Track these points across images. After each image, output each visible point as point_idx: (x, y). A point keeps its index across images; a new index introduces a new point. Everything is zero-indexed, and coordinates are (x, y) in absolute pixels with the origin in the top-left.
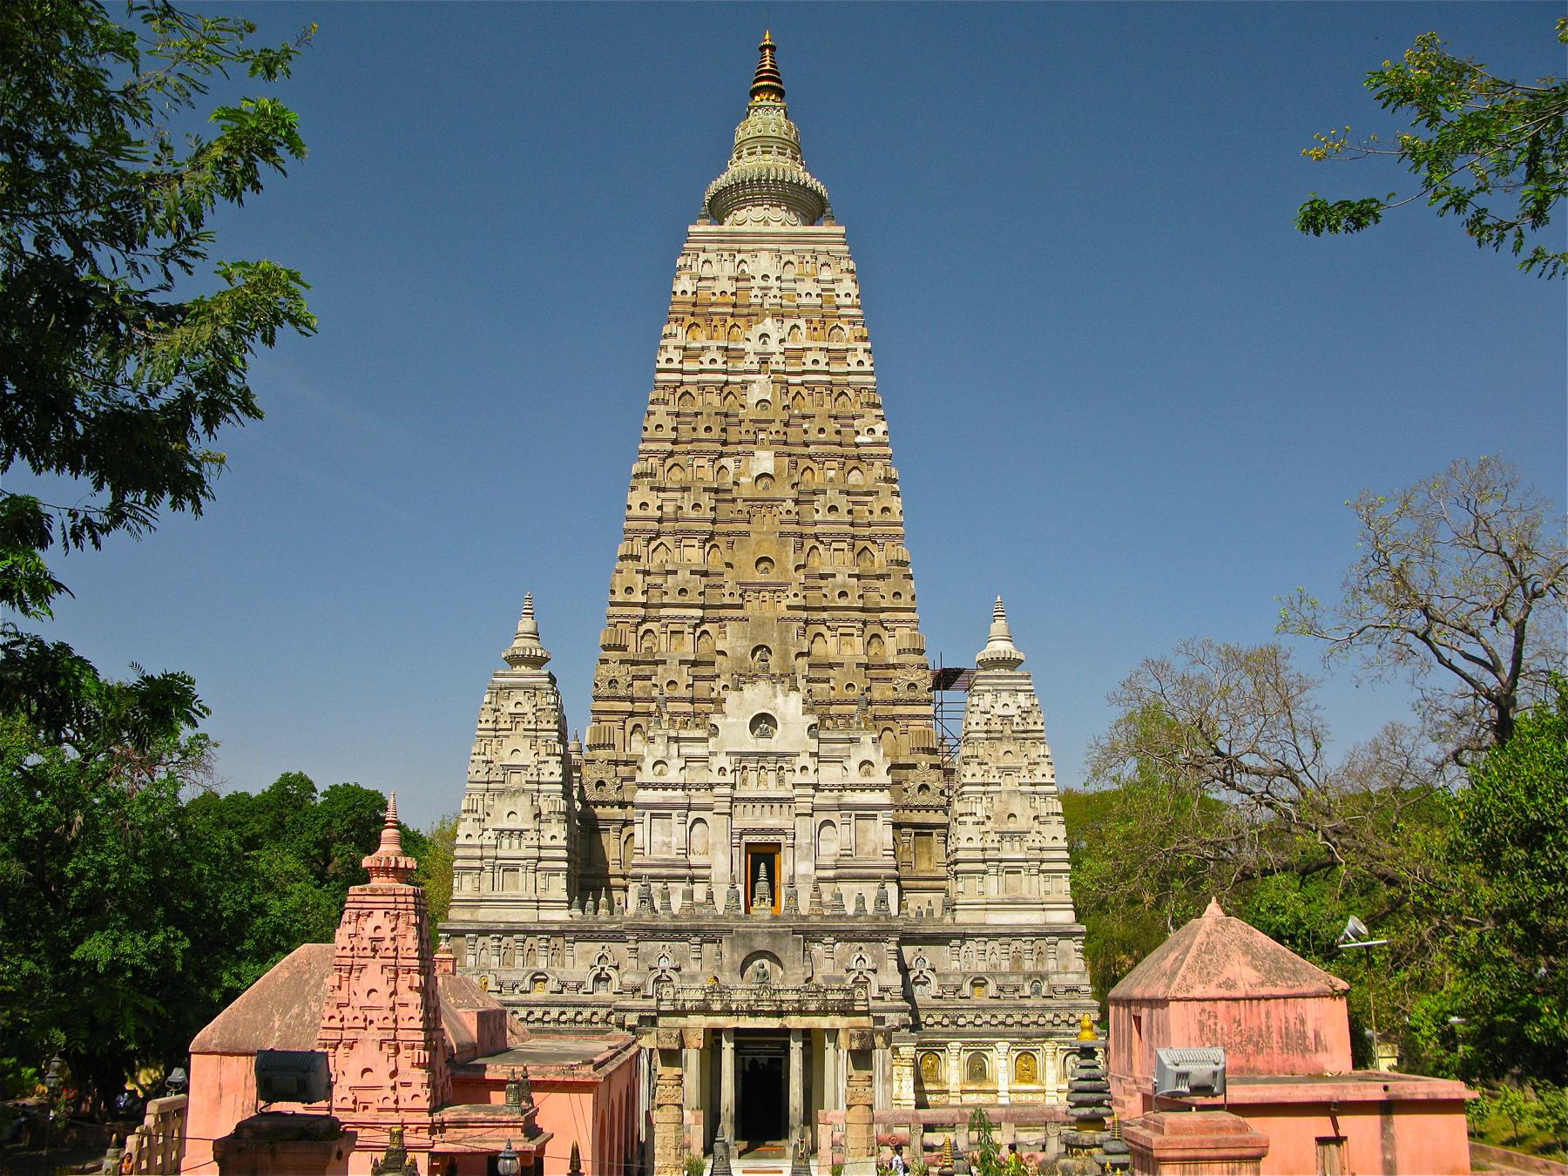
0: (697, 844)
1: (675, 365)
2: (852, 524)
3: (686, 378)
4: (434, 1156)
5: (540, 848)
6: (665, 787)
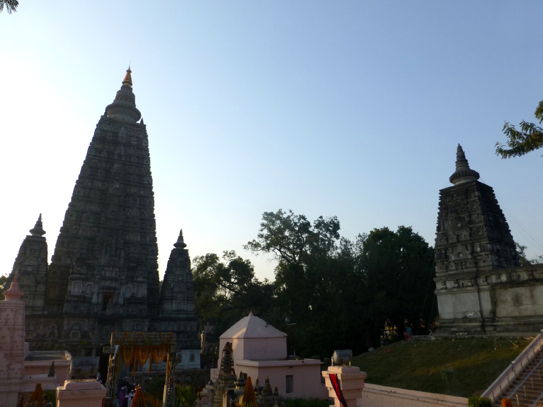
0: (88, 292)
1: (93, 154)
2: (140, 205)
3: (97, 158)
5: (36, 291)
6: (81, 274)
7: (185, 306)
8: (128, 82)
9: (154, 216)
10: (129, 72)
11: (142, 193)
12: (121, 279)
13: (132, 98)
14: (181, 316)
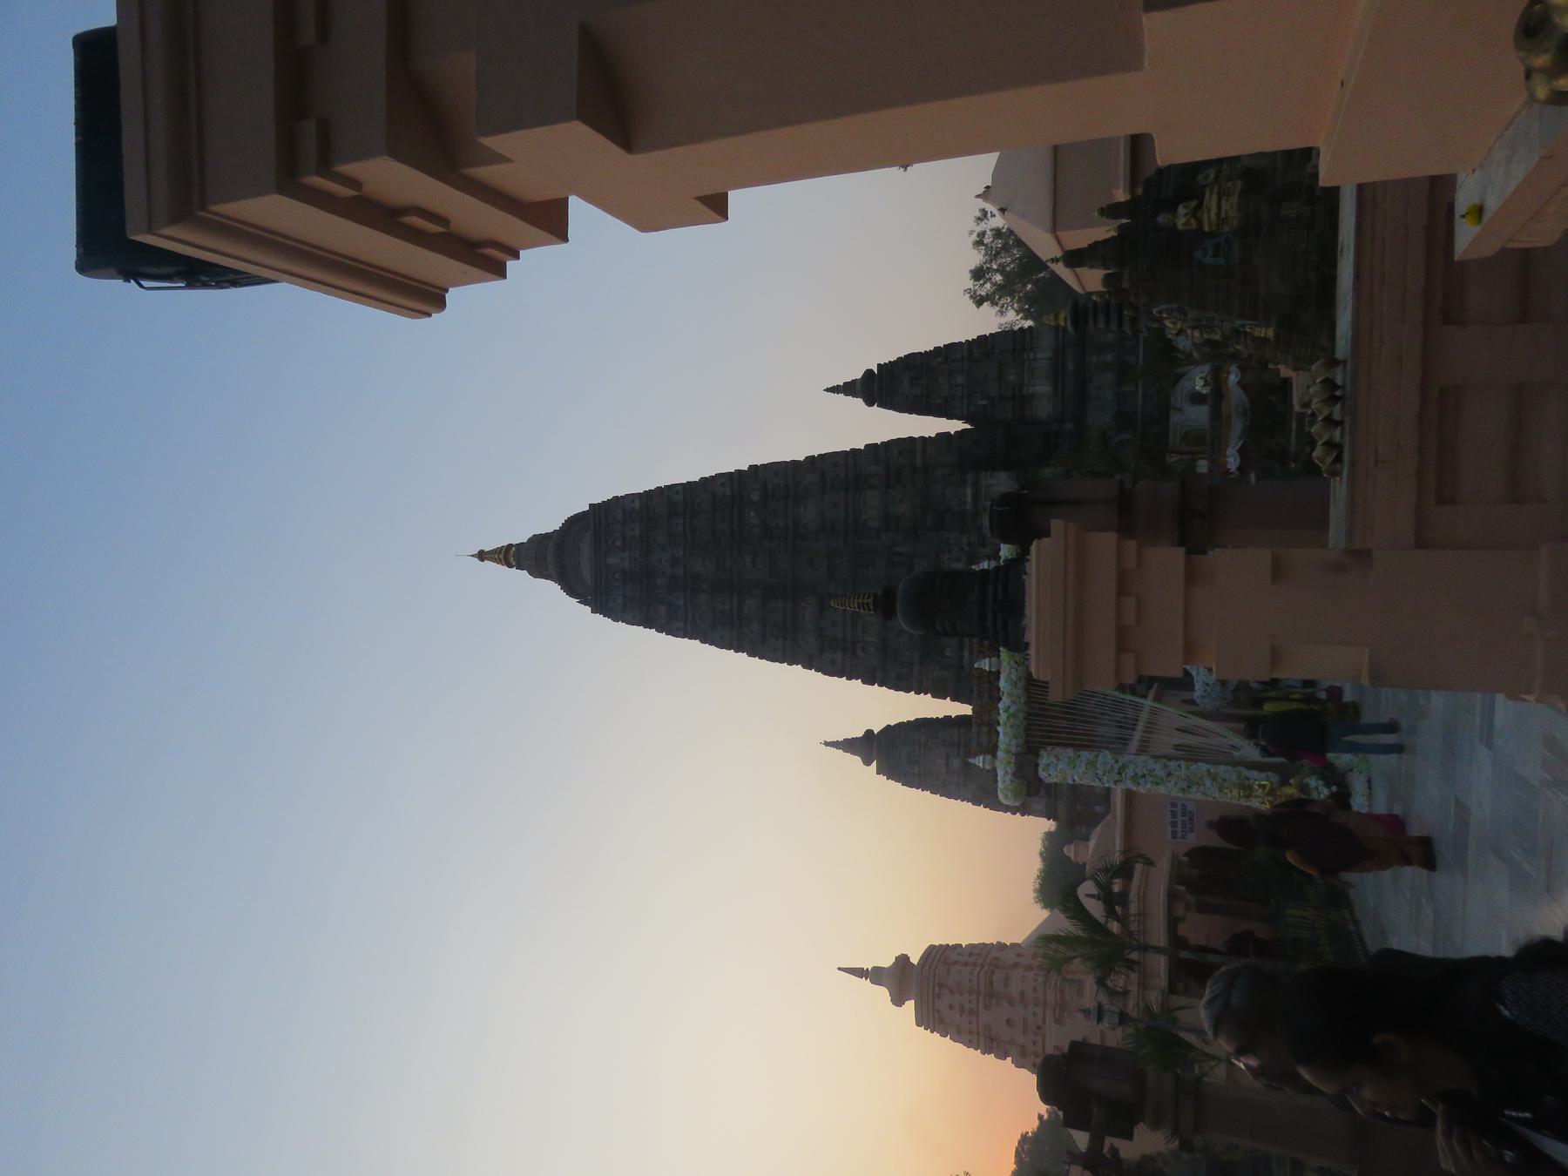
1: (681, 625)
4: (1172, 989)
7: (1039, 355)
8: (509, 556)
9: (811, 459)
10: (482, 556)
11: (755, 497)
12: (970, 544)
13: (539, 541)
14: (1070, 367)
